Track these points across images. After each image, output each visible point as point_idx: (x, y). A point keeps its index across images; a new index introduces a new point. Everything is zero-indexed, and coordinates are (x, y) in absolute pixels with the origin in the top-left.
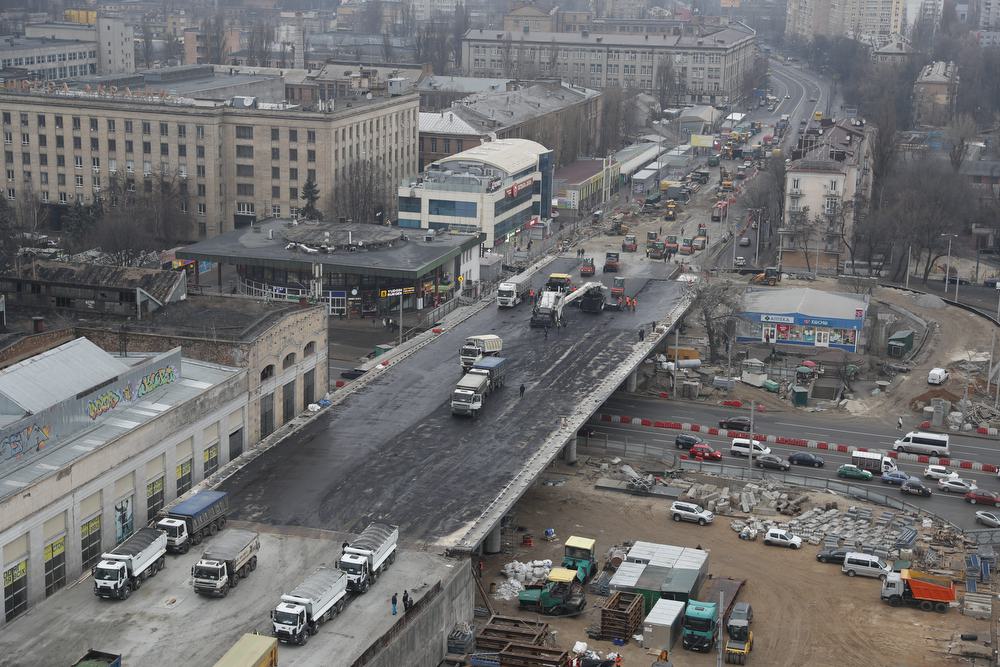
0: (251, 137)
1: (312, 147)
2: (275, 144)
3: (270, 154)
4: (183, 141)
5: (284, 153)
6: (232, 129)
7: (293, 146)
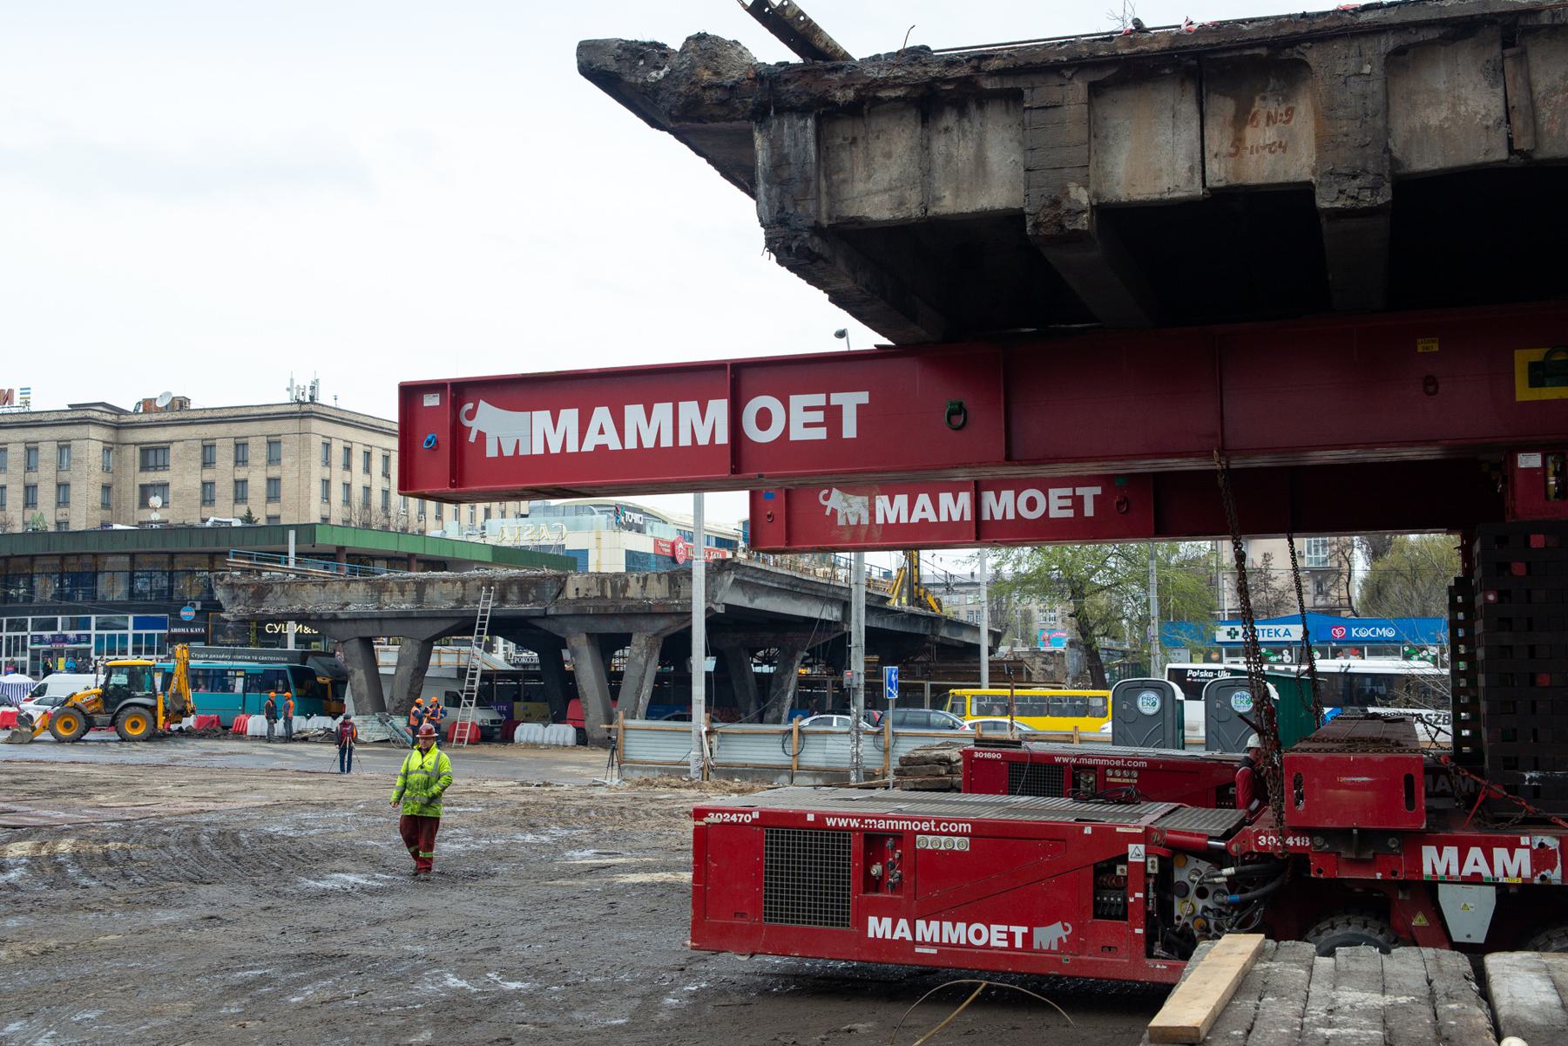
0: (165, 467)
1: (274, 472)
2: (208, 475)
3: (199, 495)
4: (33, 478)
5: (224, 490)
6: (133, 454)
7: (241, 474)
